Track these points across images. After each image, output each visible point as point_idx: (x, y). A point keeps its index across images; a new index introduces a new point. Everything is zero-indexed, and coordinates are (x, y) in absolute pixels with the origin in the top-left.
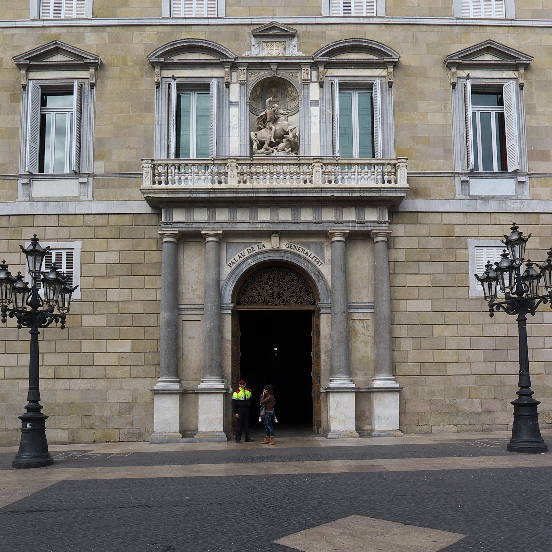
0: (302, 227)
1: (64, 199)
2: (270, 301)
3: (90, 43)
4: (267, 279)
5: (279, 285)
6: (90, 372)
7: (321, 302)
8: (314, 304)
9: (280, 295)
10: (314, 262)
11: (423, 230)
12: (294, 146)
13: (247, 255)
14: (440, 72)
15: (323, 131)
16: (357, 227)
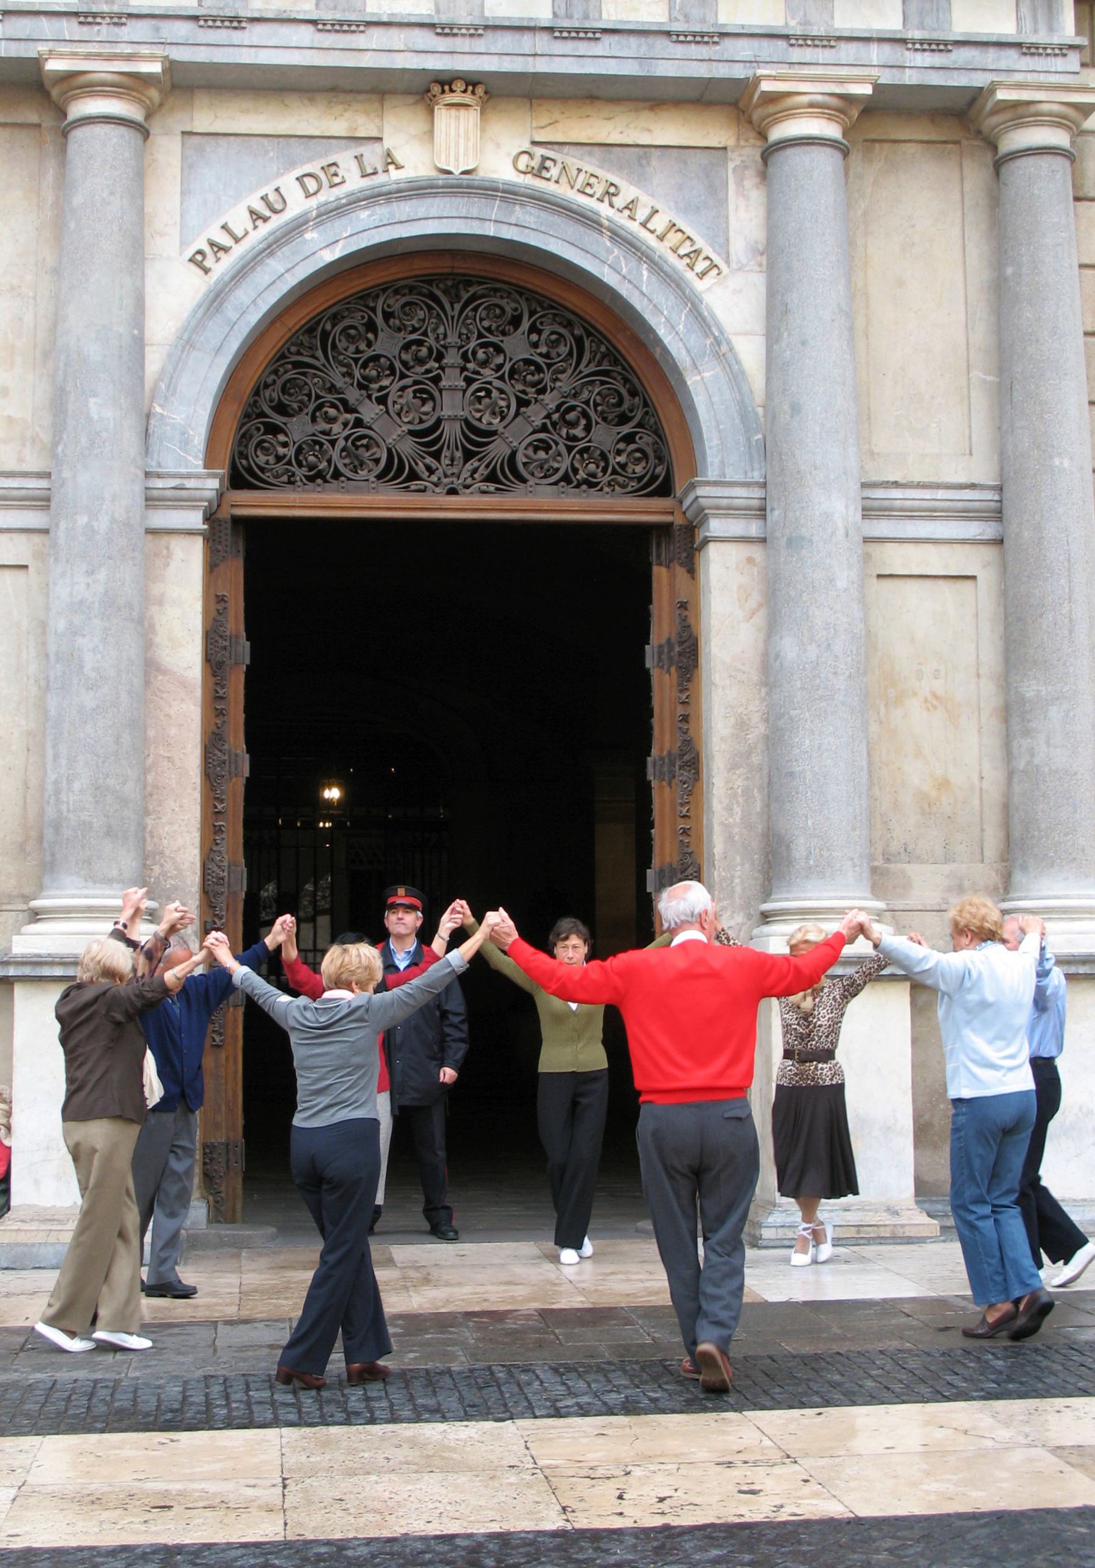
2: (420, 468)
4: (406, 347)
5: (469, 381)
7: (712, 474)
8: (665, 489)
9: (476, 439)
10: (672, 259)
13: (297, 204)
16: (918, 70)
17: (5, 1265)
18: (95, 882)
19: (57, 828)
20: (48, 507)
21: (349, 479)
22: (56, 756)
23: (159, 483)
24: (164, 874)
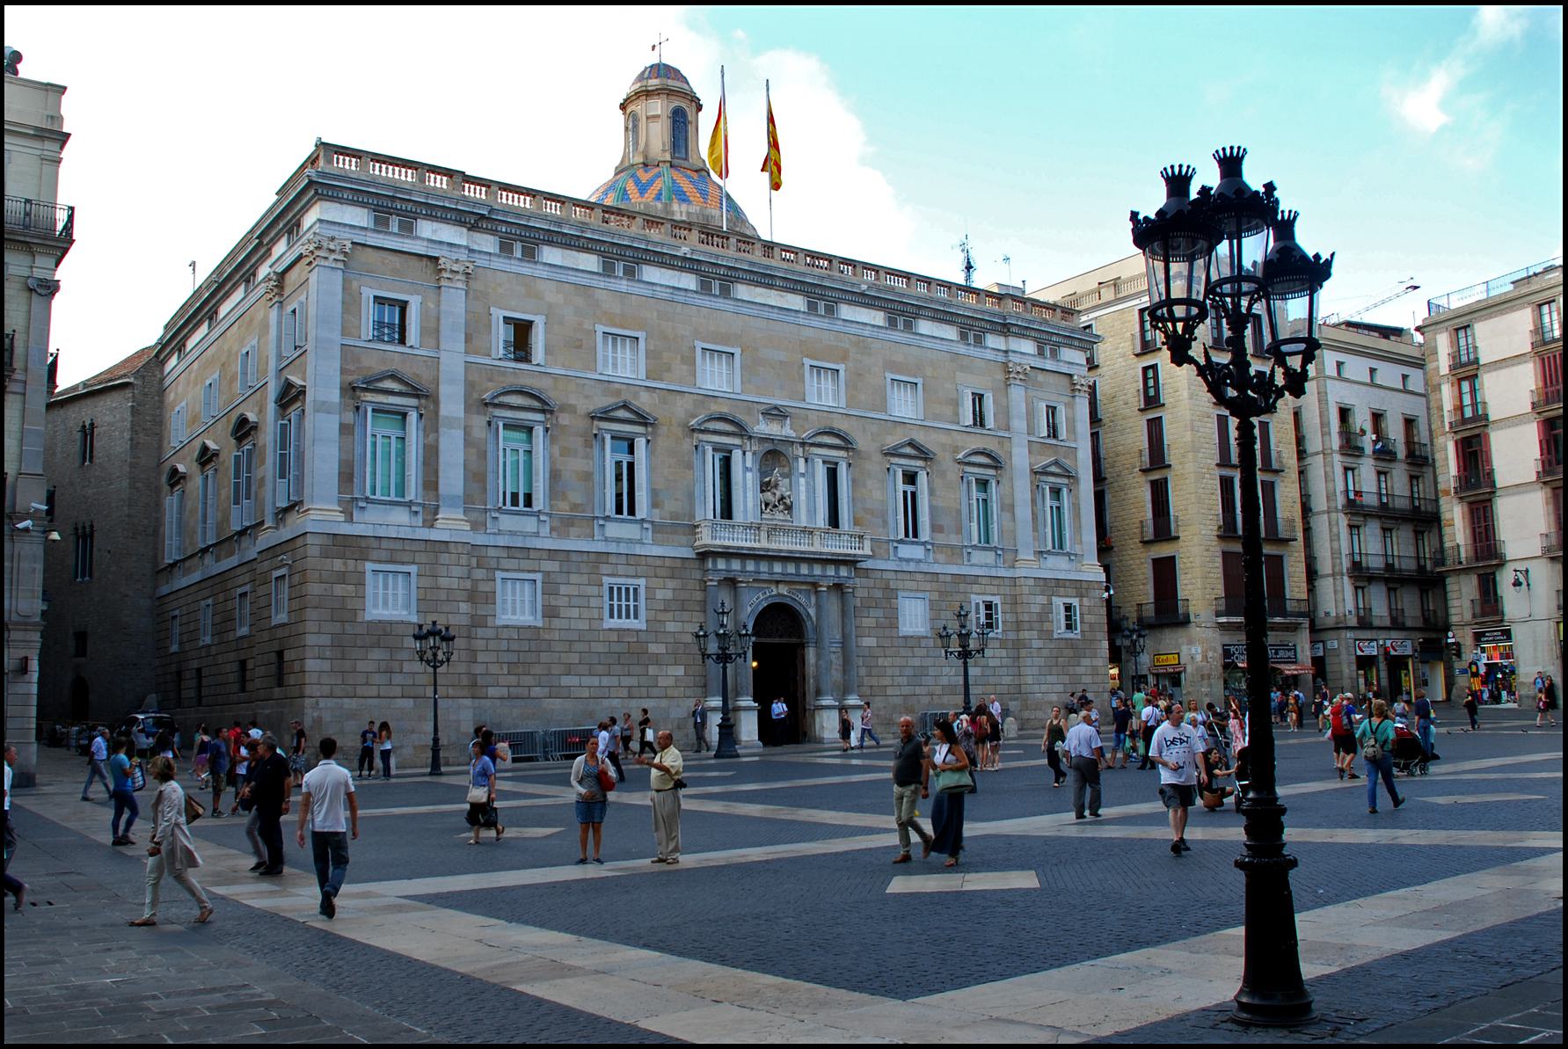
0: (801, 579)
1: (630, 541)
3: (644, 402)
6: (655, 692)
11: (871, 583)
12: (789, 508)
14: (878, 457)
15: (808, 498)
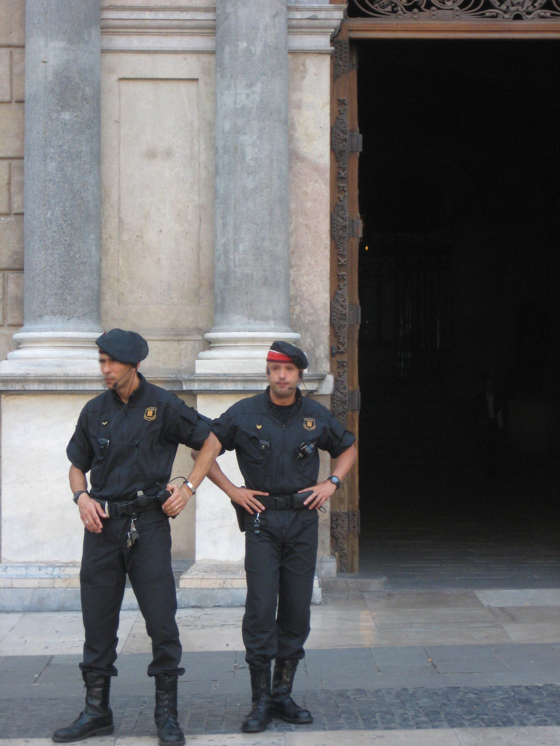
17: (193, 604)
18: (255, 320)
19: (226, 280)
20: (214, 34)
21: (439, 9)
22: (225, 225)
23: (298, 15)
24: (302, 312)
